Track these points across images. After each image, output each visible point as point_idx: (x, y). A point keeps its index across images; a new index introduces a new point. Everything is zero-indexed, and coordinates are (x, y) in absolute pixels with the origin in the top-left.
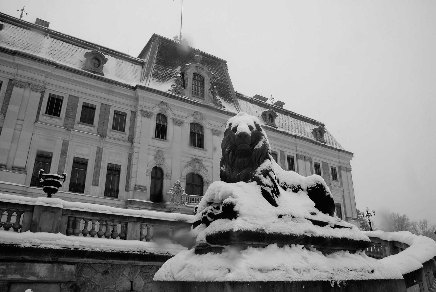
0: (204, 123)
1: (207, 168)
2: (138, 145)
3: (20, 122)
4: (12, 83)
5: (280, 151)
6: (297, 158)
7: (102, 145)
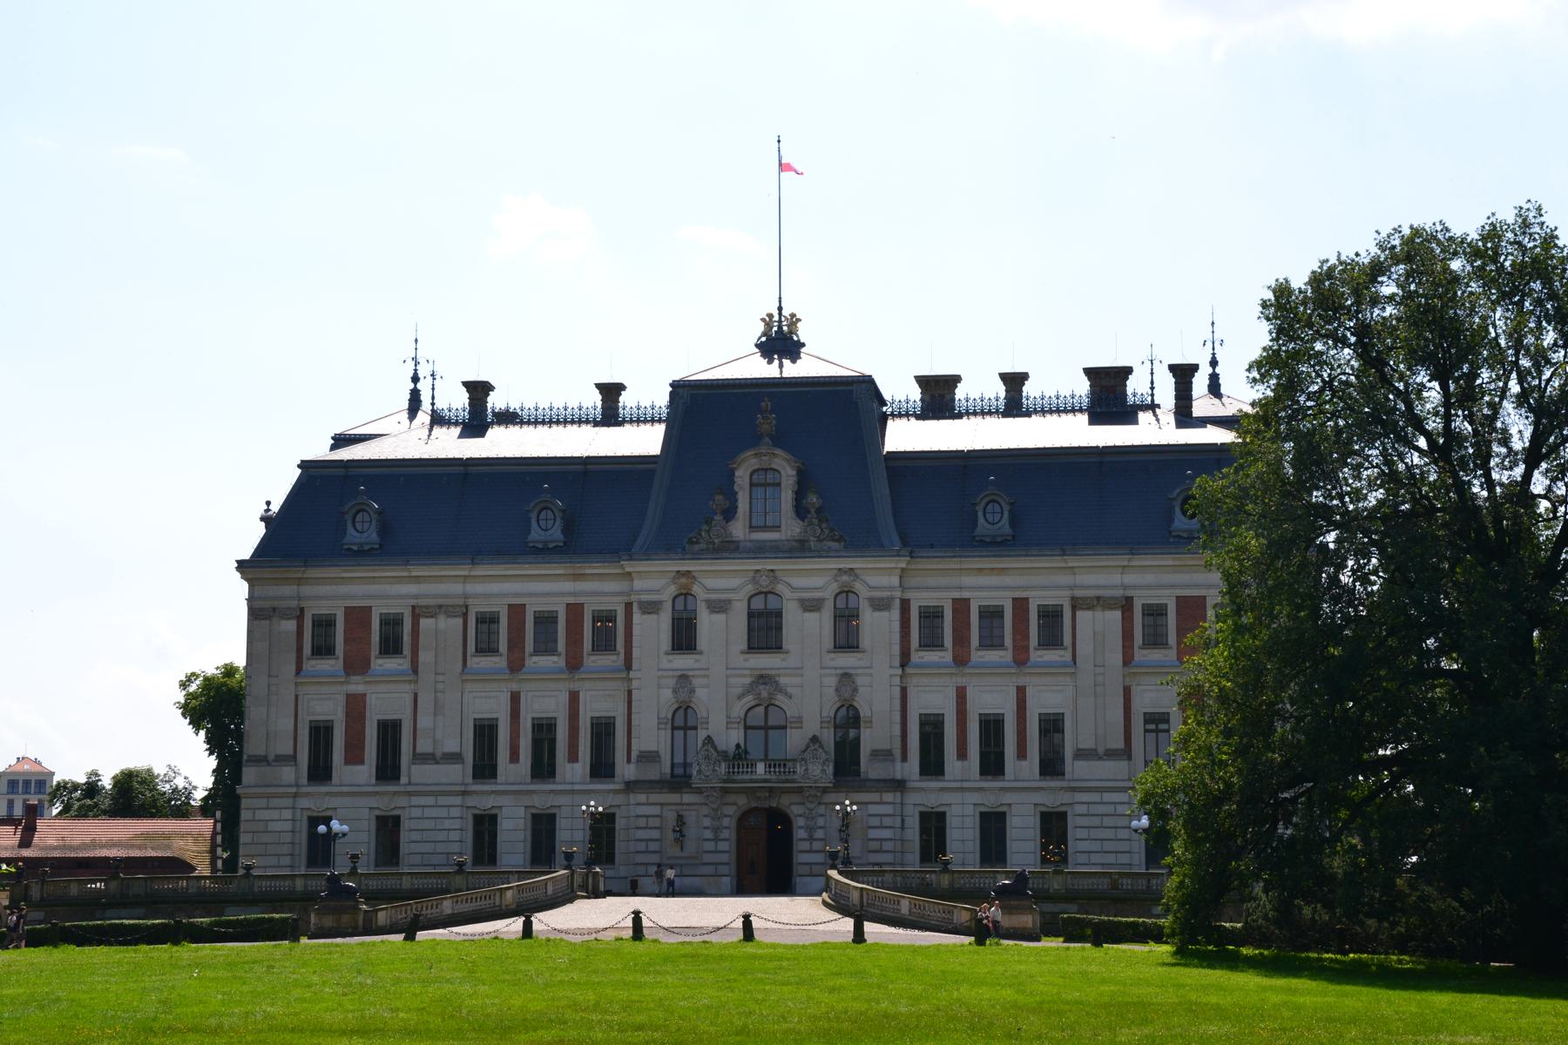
0: (780, 588)
1: (789, 690)
2: (638, 674)
3: (441, 678)
4: (417, 613)
5: (1014, 600)
6: (1074, 609)
7: (575, 686)
